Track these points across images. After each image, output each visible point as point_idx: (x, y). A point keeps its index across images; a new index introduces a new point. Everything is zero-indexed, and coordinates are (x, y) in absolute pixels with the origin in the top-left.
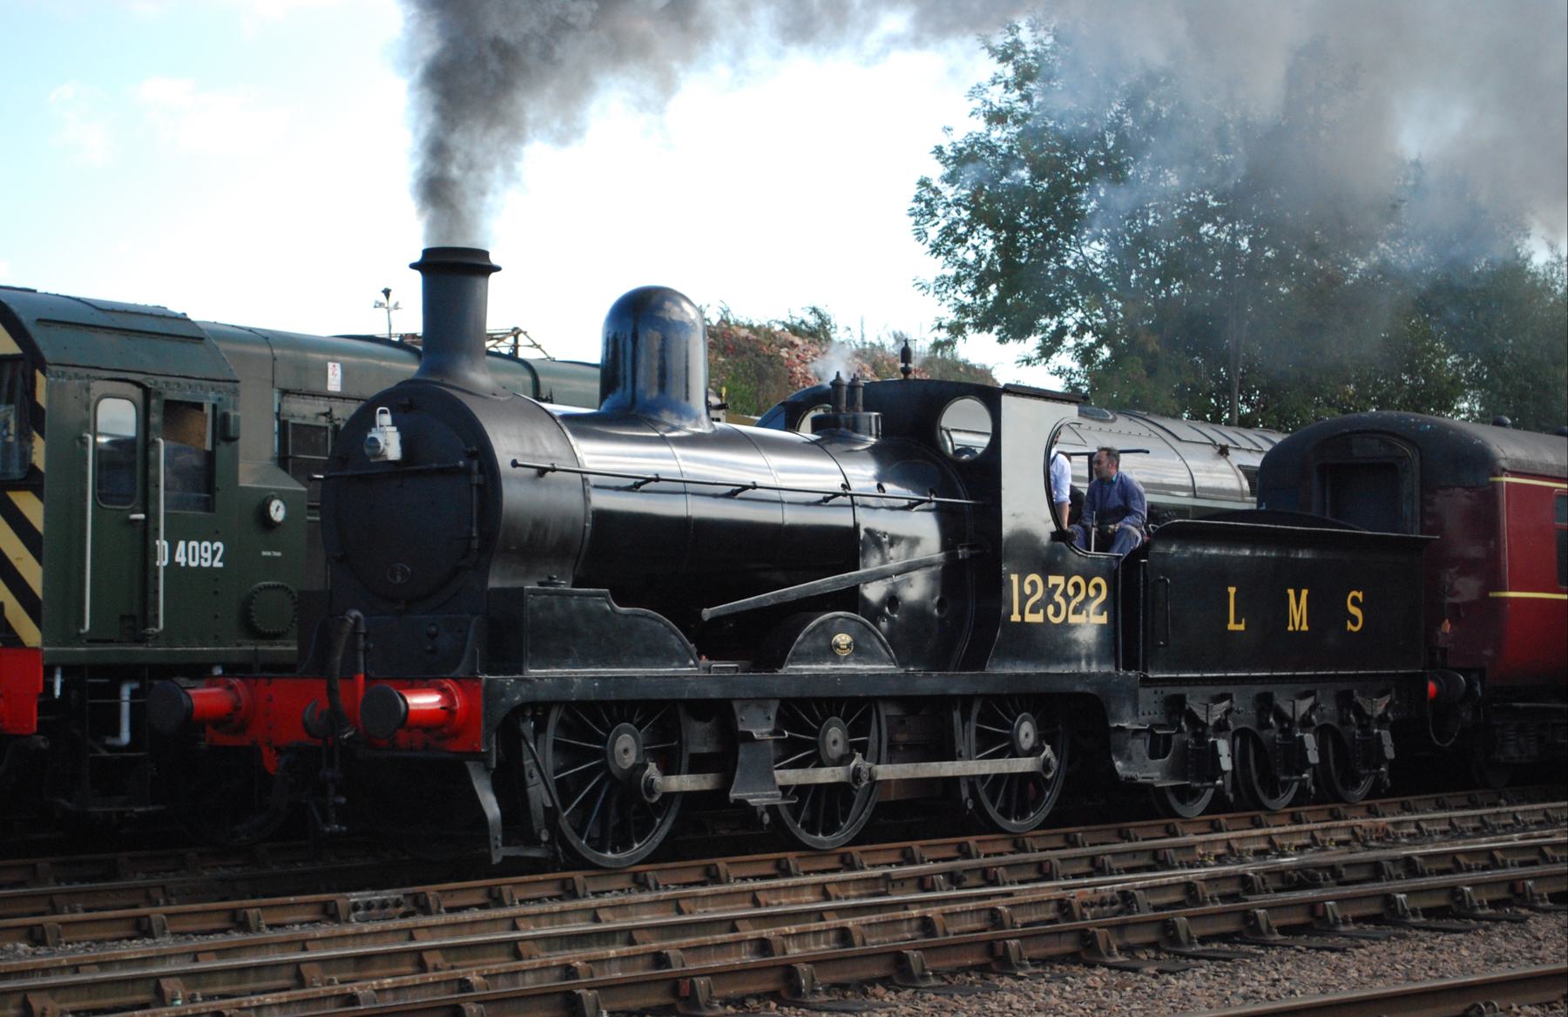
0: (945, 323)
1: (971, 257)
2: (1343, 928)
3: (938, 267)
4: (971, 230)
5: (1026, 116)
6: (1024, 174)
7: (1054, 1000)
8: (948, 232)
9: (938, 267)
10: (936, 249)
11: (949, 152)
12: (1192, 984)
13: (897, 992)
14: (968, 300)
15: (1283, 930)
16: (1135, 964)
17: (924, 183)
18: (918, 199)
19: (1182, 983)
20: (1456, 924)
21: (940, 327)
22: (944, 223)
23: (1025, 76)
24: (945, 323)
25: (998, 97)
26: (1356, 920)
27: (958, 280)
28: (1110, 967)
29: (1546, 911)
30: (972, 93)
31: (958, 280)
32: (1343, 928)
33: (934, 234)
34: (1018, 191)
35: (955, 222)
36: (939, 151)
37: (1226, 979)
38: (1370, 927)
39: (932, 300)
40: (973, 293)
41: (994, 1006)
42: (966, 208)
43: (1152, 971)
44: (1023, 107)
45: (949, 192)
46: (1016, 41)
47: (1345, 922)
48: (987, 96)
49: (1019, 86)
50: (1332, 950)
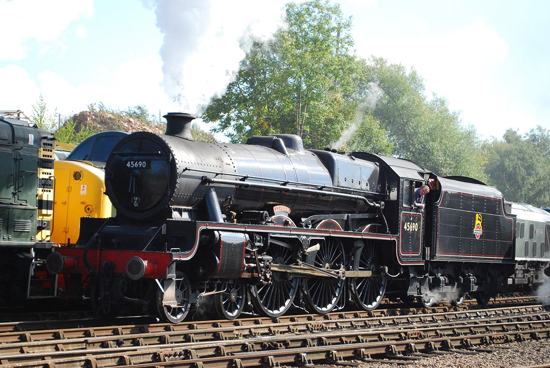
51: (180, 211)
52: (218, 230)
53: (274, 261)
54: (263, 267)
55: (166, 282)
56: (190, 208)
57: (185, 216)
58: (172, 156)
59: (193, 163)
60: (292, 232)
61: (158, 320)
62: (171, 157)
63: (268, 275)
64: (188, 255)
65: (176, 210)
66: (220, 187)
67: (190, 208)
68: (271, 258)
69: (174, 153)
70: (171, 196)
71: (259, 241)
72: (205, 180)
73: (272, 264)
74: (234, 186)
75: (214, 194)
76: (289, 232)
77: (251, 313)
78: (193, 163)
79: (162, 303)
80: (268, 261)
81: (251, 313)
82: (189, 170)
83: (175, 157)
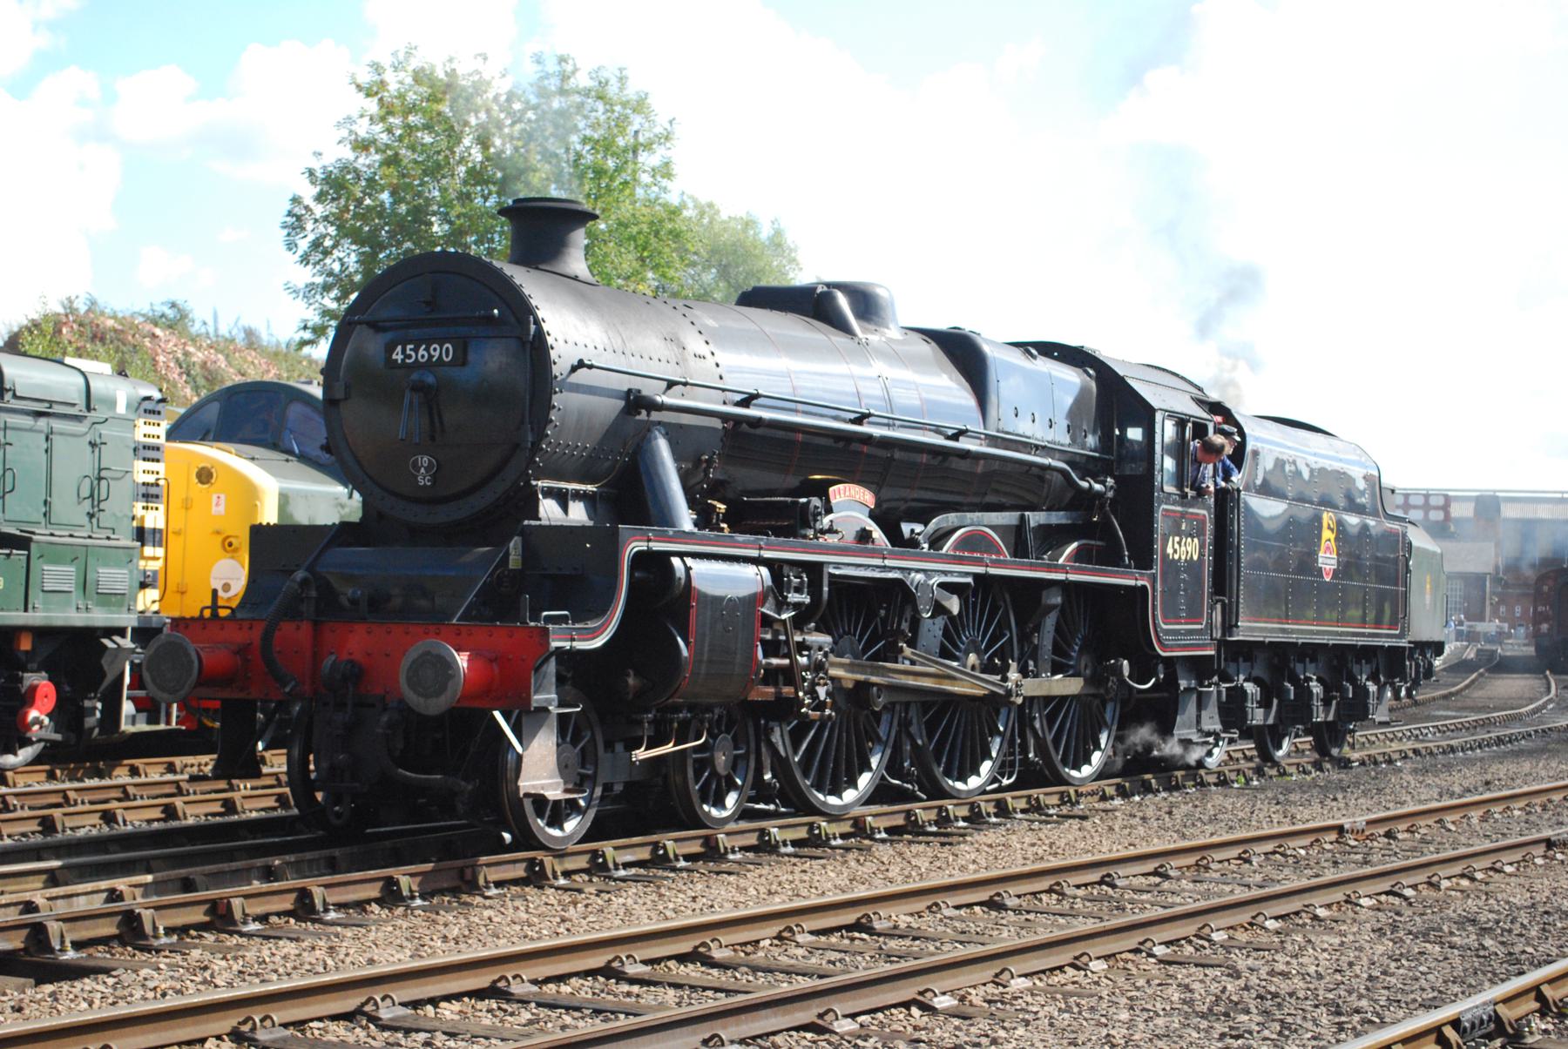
0: (310, 324)
1: (336, 267)
2: (731, 857)
3: (307, 275)
4: (335, 246)
5: (387, 146)
6: (385, 196)
7: (524, 916)
8: (316, 244)
9: (307, 275)
10: (305, 259)
11: (319, 174)
12: (630, 901)
13: (390, 910)
14: (334, 306)
15: (687, 858)
16: (576, 886)
17: (296, 200)
18: (290, 214)
19: (621, 900)
20: (819, 852)
21: (305, 328)
22: (311, 237)
23: (387, 111)
24: (310, 324)
25: (363, 129)
26: (742, 849)
27: (326, 288)
28: (557, 888)
29: (883, 841)
30: (339, 125)
31: (326, 288)
32: (731, 857)
33: (304, 245)
34: (379, 210)
35: (324, 236)
36: (311, 173)
37: (654, 897)
38: (750, 855)
39: (301, 303)
40: (338, 299)
41: (477, 920)
42: (332, 224)
43: (593, 890)
44: (384, 138)
45: (319, 210)
46: (382, 82)
47: (733, 852)
48: (354, 127)
49: (383, 119)
50: (730, 873)
51: (563, 499)
52: (681, 555)
53: (836, 650)
54: (807, 668)
55: (526, 719)
56: (590, 488)
57: (578, 514)
58: (537, 322)
59: (600, 347)
60: (888, 563)
61: (507, 836)
62: (533, 327)
63: (822, 692)
64: (595, 633)
65: (549, 493)
66: (681, 426)
67: (590, 488)
68: (829, 639)
69: (540, 314)
70: (536, 448)
71: (798, 590)
72: (635, 402)
73: (832, 658)
74: (717, 423)
75: (663, 447)
76: (878, 562)
77: (772, 807)
78: (600, 347)
79: (518, 788)
80: (820, 649)
81: (772, 807)
82: (591, 367)
83: (545, 327)
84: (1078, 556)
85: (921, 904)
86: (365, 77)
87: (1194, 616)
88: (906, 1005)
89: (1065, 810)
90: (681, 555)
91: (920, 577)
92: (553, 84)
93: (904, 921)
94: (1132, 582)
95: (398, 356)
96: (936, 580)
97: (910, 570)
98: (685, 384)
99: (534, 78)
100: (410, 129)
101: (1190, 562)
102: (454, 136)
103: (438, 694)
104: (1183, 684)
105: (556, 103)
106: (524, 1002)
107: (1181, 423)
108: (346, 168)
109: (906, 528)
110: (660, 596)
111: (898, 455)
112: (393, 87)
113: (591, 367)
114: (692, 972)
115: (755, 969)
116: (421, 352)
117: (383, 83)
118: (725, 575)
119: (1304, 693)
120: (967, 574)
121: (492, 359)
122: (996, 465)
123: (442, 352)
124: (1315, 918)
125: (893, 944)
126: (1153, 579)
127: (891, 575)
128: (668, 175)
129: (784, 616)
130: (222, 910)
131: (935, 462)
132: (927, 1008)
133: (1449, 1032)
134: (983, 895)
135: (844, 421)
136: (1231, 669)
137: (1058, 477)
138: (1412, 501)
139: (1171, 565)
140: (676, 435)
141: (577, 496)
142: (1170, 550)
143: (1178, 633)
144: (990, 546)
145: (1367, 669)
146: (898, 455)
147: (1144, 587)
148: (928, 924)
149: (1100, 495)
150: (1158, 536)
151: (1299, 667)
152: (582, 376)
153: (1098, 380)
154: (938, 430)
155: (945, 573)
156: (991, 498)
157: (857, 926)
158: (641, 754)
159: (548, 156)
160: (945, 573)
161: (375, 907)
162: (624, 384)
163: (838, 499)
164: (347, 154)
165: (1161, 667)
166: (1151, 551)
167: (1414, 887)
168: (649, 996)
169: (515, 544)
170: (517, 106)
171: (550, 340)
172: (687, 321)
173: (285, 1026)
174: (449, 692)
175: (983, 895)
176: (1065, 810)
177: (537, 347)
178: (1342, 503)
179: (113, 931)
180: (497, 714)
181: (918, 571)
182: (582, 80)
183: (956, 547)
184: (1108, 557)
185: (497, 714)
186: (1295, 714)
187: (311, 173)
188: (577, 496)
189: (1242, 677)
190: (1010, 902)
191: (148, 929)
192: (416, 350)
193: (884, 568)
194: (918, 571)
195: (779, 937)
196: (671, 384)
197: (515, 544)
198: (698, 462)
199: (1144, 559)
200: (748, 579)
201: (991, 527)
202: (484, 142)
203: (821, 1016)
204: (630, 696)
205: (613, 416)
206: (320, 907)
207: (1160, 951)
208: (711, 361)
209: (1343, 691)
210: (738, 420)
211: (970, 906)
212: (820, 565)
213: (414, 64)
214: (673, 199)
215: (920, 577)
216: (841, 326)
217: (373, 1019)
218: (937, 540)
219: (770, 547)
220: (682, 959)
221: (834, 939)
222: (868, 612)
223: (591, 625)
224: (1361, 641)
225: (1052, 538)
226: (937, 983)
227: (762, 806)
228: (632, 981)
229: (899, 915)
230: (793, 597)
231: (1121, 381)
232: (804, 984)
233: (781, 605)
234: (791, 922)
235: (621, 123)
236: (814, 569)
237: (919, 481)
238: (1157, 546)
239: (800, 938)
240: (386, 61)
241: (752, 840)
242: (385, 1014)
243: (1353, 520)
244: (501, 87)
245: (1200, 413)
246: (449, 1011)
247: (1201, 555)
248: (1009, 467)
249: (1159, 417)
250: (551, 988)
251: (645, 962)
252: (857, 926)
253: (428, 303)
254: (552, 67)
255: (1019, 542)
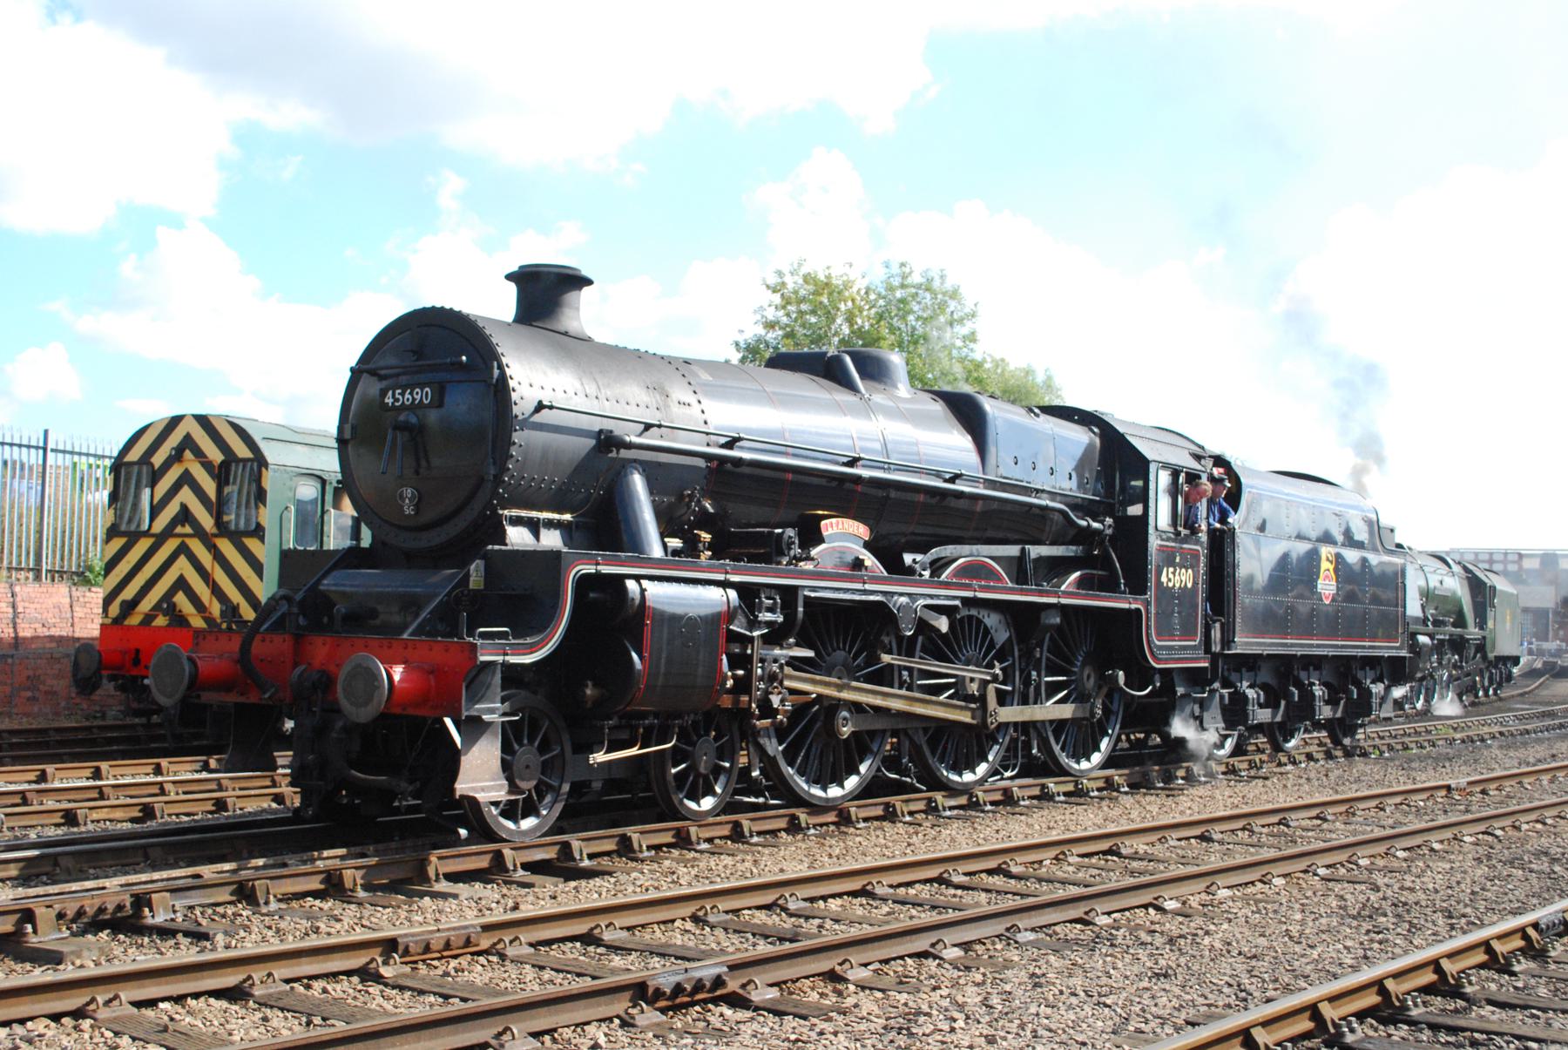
51: (534, 527)
52: (637, 578)
55: (474, 728)
56: (567, 517)
58: (500, 367)
60: (867, 587)
62: (496, 372)
64: (532, 649)
65: (517, 521)
66: (659, 464)
67: (567, 517)
69: (504, 360)
70: (498, 480)
71: (771, 610)
72: (607, 442)
74: (701, 463)
75: (638, 482)
76: (859, 586)
77: (761, 800)
78: (571, 393)
79: (453, 790)
81: (761, 800)
82: (551, 407)
83: (508, 372)
84: (1081, 583)
85: (1154, 837)
86: (773, 280)
87: (1188, 633)
88: (1146, 906)
89: (1253, 773)
90: (637, 578)
91: (904, 600)
92: (896, 282)
93: (1142, 848)
94: (1126, 606)
95: (389, 400)
96: (921, 602)
97: (893, 594)
98: (660, 426)
99: (884, 277)
100: (801, 313)
101: (1184, 589)
102: (831, 319)
103: (366, 704)
104: (1180, 690)
105: (898, 294)
106: (884, 900)
107: (1175, 473)
108: (759, 340)
109: (908, 558)
110: (608, 615)
111: (893, 494)
112: (790, 286)
113: (551, 407)
114: (997, 881)
115: (1040, 880)
116: (407, 396)
117: (783, 284)
118: (684, 594)
119: (1307, 697)
120: (955, 598)
121: (462, 404)
122: (995, 506)
123: (422, 395)
124: (1432, 850)
125: (1135, 864)
126: (1147, 604)
127: (872, 598)
128: (974, 341)
129: (756, 634)
130: (684, 835)
131: (934, 501)
132: (1159, 909)
133: (1531, 932)
134: (1197, 831)
135: (837, 463)
136: (1234, 677)
137: (1057, 516)
138: (1495, 557)
139: (1163, 591)
140: (654, 473)
141: (550, 524)
142: (1164, 579)
143: (1170, 649)
144: (990, 574)
145: (1371, 674)
146: (893, 494)
147: (1138, 610)
148: (1159, 850)
149: (1097, 532)
150: (1152, 567)
151: (1303, 675)
152: (544, 416)
153: (1102, 436)
154: (938, 474)
155: (931, 597)
156: (990, 534)
157: (1109, 852)
158: (600, 757)
159: (892, 330)
160: (931, 597)
161: (783, 834)
162: (597, 425)
163: (830, 531)
164: (761, 331)
165: (1157, 677)
166: (1145, 580)
167: (1503, 829)
168: (968, 898)
169: (476, 570)
170: (872, 297)
171: (512, 384)
172: (679, 374)
173: (727, 912)
174: (376, 700)
175: (1197, 831)
176: (1253, 773)
177: (501, 389)
178: (1340, 538)
179: (613, 847)
180: (448, 721)
181: (901, 594)
182: (916, 279)
183: (957, 573)
184: (1109, 585)
185: (448, 721)
186: (1302, 713)
187: (737, 344)
188: (550, 524)
189: (1245, 684)
190: (1215, 837)
191: (636, 846)
192: (403, 394)
193: (865, 592)
194: (901, 594)
195: (1056, 858)
196: (648, 427)
197: (476, 570)
198: (681, 497)
199: (1138, 585)
200: (713, 598)
201: (992, 558)
202: (850, 320)
203: (1086, 913)
204: (589, 705)
205: (584, 453)
206: (747, 834)
207: (1322, 871)
208: (696, 408)
209: (1348, 693)
210: (723, 460)
211: (1187, 839)
212: (796, 588)
213: (804, 271)
214: (978, 356)
215: (904, 600)
216: (849, 385)
217: (784, 909)
218: (937, 566)
219: (736, 572)
220: (990, 872)
221: (1094, 860)
222: (845, 632)
223: (529, 640)
224: (1360, 652)
225: (1057, 567)
226: (1166, 892)
227: (753, 800)
228: (957, 887)
229: (1139, 845)
230: (766, 616)
231: (1121, 437)
232: (1074, 891)
233: (753, 624)
234: (1065, 848)
235: (942, 306)
236: (789, 593)
237: (908, 516)
238: (1152, 576)
239: (1070, 859)
240: (786, 271)
241: (1036, 791)
242: (792, 906)
243: (1352, 556)
244: (860, 285)
245: (1193, 464)
246: (834, 904)
247: (1195, 583)
248: (1009, 507)
249: (1153, 468)
250: (902, 891)
251: (966, 874)
252: (1109, 852)
253: (414, 352)
254: (895, 270)
255: (1020, 571)
